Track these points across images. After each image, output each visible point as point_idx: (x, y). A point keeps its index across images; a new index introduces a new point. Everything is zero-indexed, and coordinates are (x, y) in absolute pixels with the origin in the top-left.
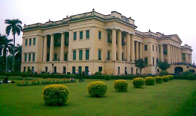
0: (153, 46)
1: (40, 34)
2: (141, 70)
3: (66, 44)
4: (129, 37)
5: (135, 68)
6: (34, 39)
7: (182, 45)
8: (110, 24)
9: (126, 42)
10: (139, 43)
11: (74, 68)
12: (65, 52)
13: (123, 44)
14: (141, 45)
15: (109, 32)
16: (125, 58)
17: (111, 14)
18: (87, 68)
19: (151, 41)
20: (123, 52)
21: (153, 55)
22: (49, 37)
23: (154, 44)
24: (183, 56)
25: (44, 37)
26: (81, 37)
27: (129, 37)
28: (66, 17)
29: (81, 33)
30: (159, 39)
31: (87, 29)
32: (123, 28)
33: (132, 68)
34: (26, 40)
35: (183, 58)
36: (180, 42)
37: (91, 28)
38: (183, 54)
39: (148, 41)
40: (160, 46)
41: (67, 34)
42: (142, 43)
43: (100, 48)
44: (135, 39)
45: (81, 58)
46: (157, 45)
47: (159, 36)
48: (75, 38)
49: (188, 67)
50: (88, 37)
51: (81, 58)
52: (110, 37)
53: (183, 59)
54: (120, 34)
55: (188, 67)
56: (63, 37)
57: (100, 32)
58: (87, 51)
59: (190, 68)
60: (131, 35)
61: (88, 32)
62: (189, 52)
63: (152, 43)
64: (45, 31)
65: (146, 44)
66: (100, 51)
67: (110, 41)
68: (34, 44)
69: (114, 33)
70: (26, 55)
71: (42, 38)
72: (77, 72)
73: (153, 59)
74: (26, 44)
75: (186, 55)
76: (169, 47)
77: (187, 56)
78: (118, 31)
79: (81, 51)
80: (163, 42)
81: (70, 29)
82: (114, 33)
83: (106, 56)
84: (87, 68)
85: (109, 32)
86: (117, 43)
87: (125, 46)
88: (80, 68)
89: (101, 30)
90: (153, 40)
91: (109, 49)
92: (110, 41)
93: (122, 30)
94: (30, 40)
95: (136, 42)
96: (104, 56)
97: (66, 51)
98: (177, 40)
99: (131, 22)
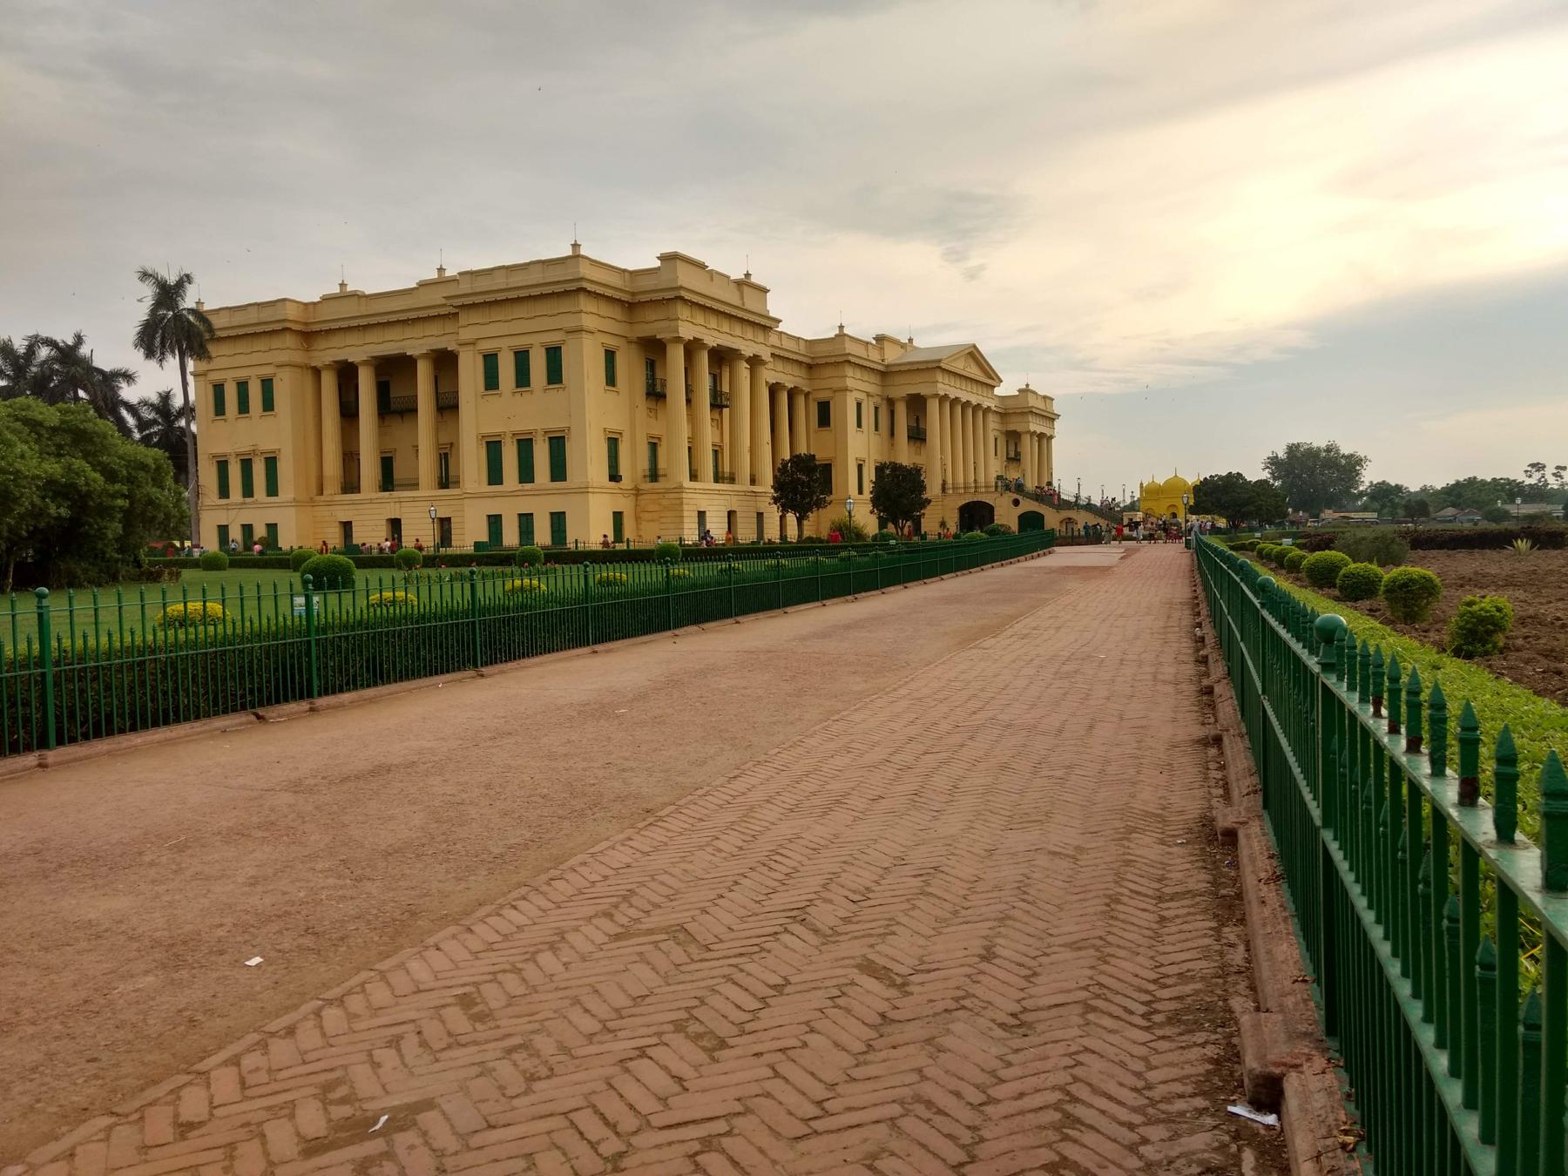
0: (859, 405)
1: (298, 357)
2: (800, 521)
3: (447, 407)
4: (743, 370)
5: (773, 514)
6: (267, 384)
7: (998, 391)
8: (651, 315)
9: (731, 396)
10: (792, 394)
11: (495, 522)
12: (439, 446)
13: (717, 404)
14: (801, 401)
15: (653, 350)
16: (727, 469)
17: (658, 263)
18: (558, 520)
19: (850, 383)
20: (717, 440)
21: (859, 449)
22: (346, 374)
23: (862, 396)
24: (1012, 448)
25: (317, 372)
26: (523, 379)
27: (743, 370)
28: (435, 275)
29: (522, 358)
30: (886, 374)
31: (553, 339)
32: (715, 335)
33: (760, 515)
34: (219, 390)
35: (1012, 455)
36: (989, 378)
37: (571, 336)
38: (1013, 437)
39: (836, 384)
40: (891, 402)
41: (445, 362)
42: (807, 395)
43: (614, 425)
44: (771, 374)
45: (526, 474)
46: (877, 400)
47: (892, 356)
48: (491, 382)
49: (1016, 503)
50: (555, 374)
51: (526, 474)
52: (659, 375)
53: (1009, 459)
54: (704, 359)
55: (1016, 503)
56: (424, 371)
57: (610, 356)
58: (557, 444)
59: (1027, 506)
60: (755, 362)
61: (554, 356)
62: (1036, 426)
63: (858, 389)
64: (321, 344)
65: (823, 396)
66: (613, 444)
67: (656, 394)
68: (268, 405)
69: (677, 356)
70: (223, 466)
71: (309, 379)
72: (511, 538)
73: (860, 467)
74: (220, 409)
75: (1026, 440)
76: (933, 407)
77: (1028, 448)
78: (692, 348)
79: (525, 447)
80: (902, 389)
81: (466, 334)
82: (677, 356)
83: (644, 464)
84: (558, 520)
85: (653, 350)
86: (689, 401)
87: (726, 411)
88: (526, 521)
89: (612, 342)
90: (858, 374)
91: (655, 432)
92: (656, 394)
93: (712, 340)
94: (242, 386)
95: (774, 390)
96: (633, 462)
97: (444, 439)
98: (974, 371)
99: (751, 303)
